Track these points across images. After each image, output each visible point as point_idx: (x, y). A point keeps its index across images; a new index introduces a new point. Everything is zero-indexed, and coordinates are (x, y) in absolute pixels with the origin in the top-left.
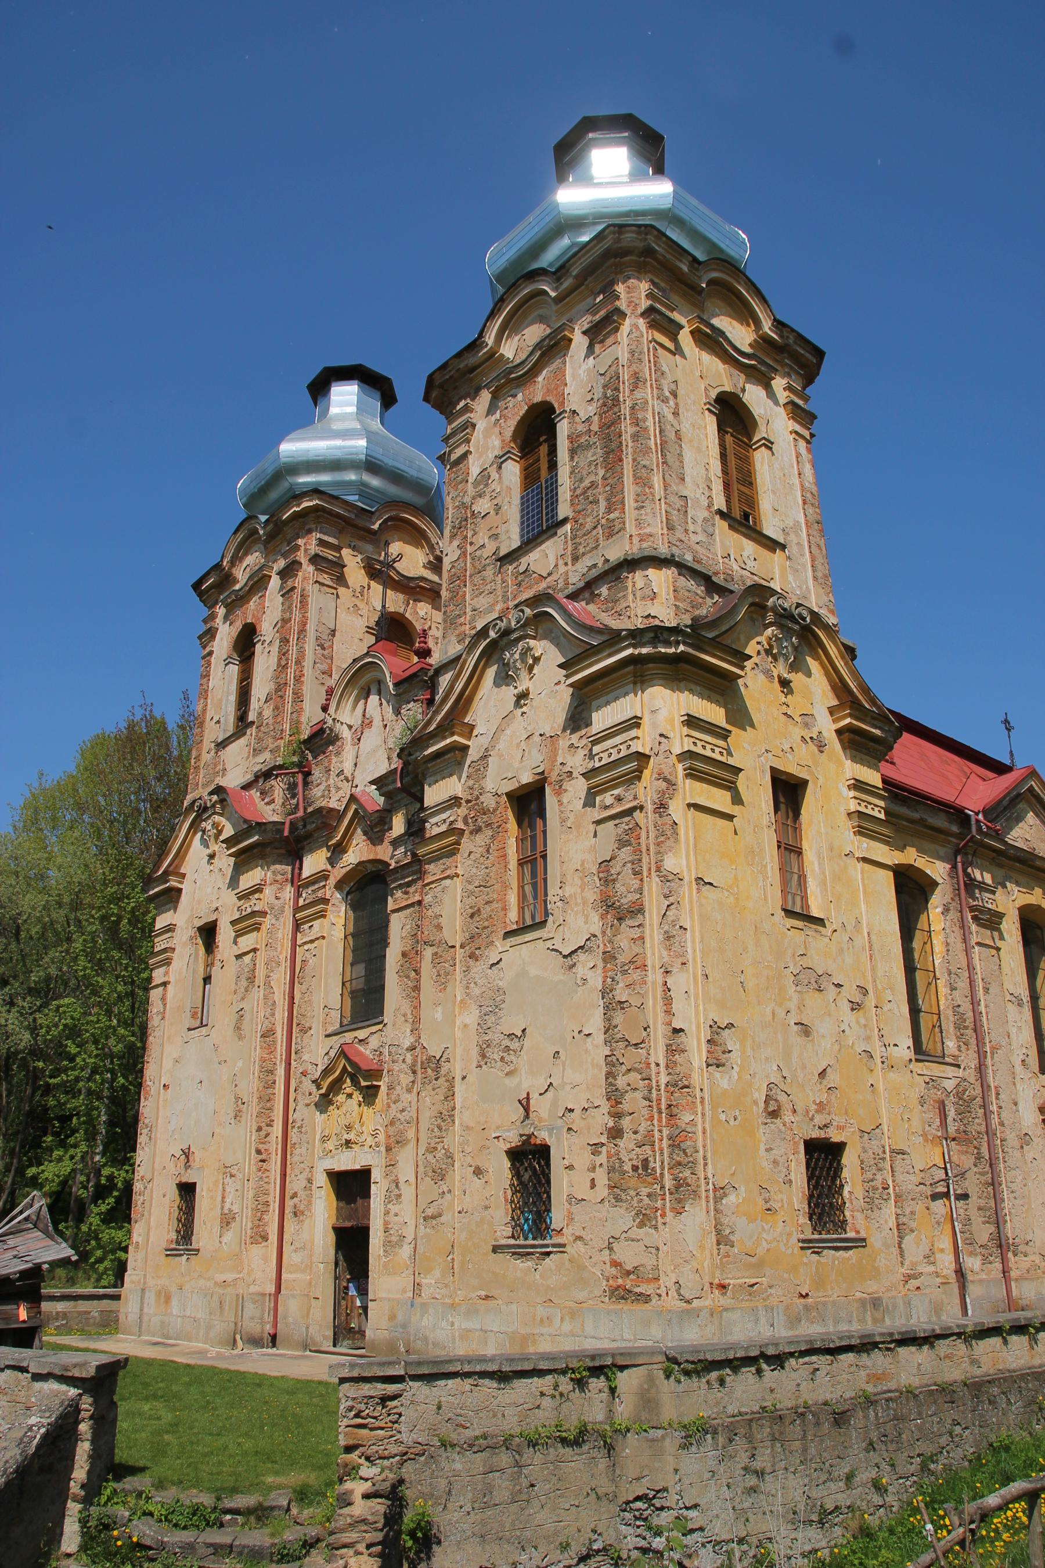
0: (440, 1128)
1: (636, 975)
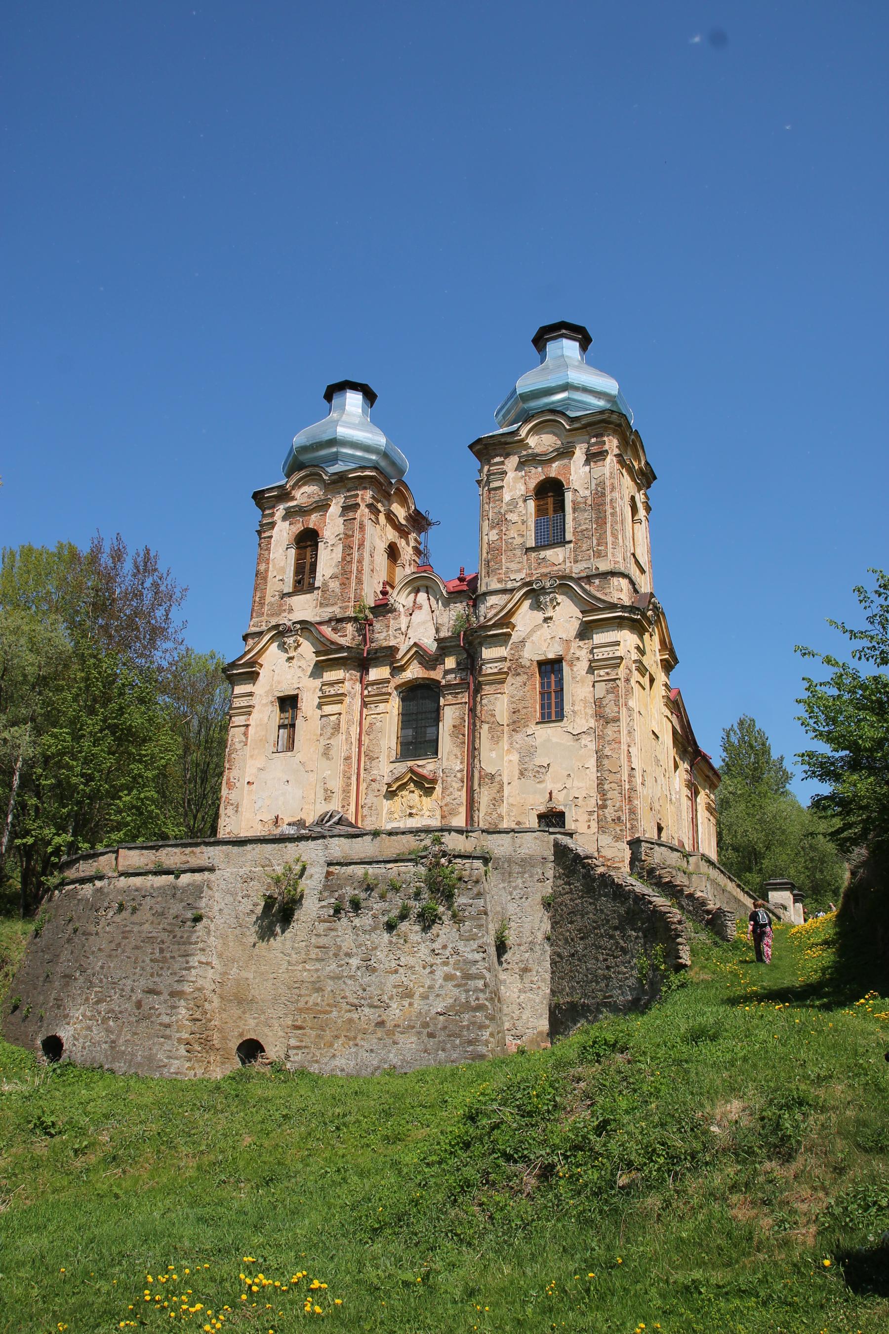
1: (616, 746)
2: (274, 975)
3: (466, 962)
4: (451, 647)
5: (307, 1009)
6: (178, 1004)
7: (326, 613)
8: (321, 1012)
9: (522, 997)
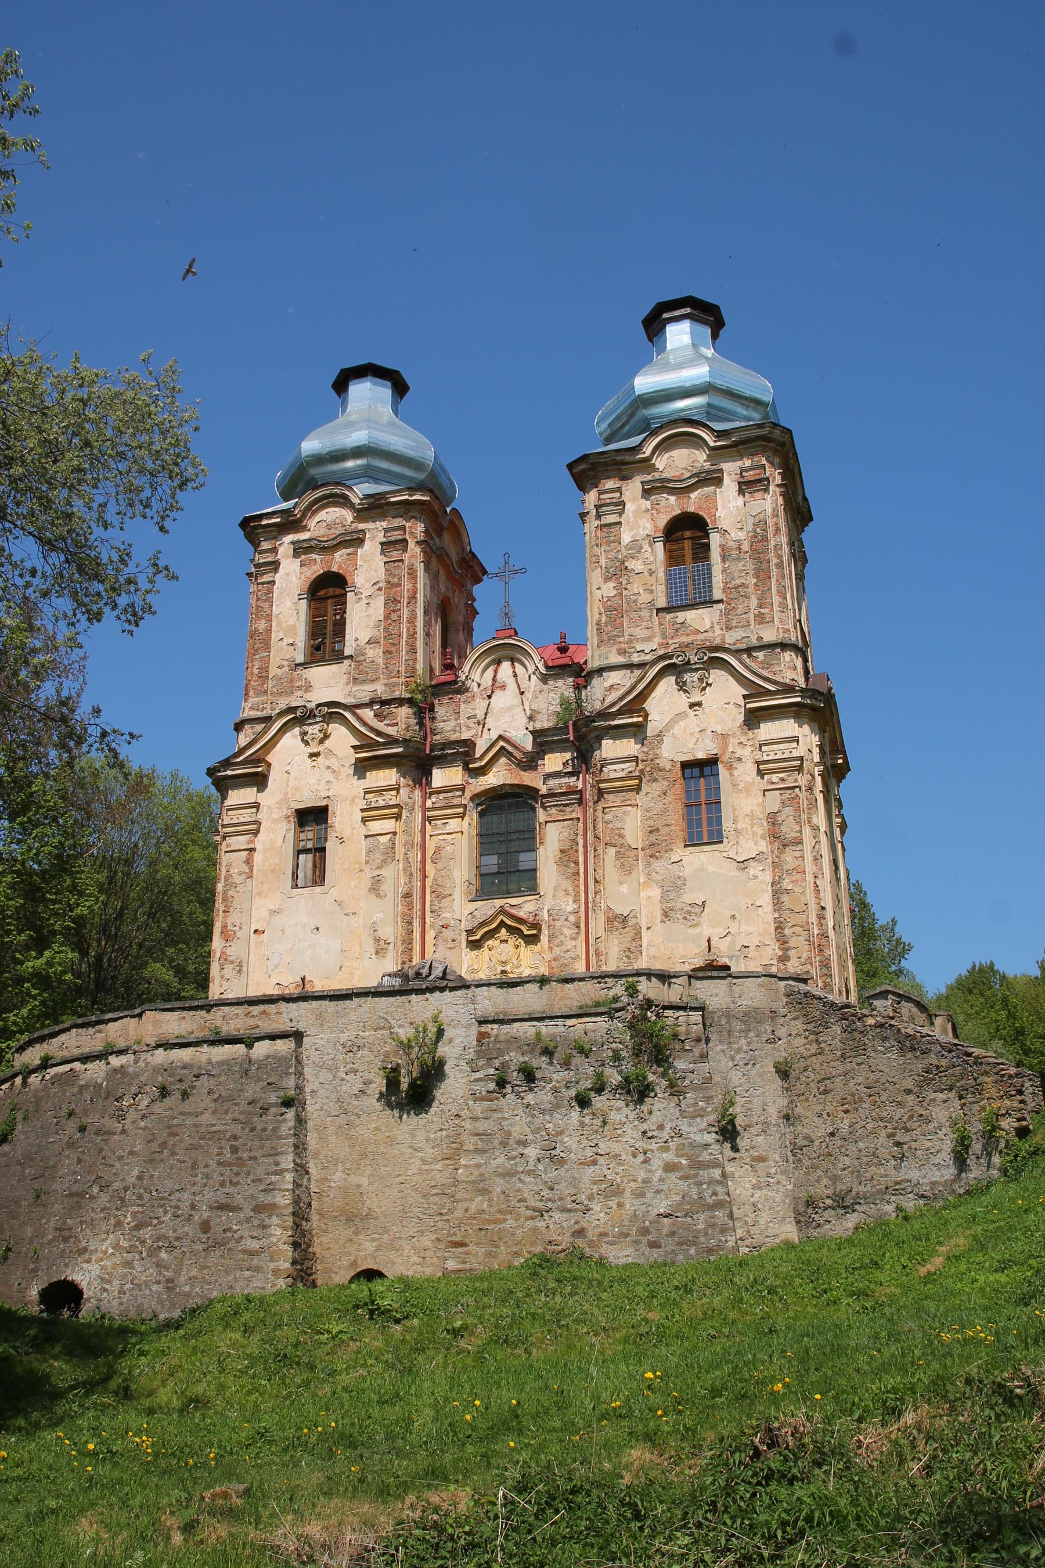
0: (628, 957)
2: (400, 1179)
3: (693, 1145)
4: (554, 742)
5: (469, 1218)
6: (267, 1222)
7: (365, 692)
8: (489, 1222)
9: (757, 1195)
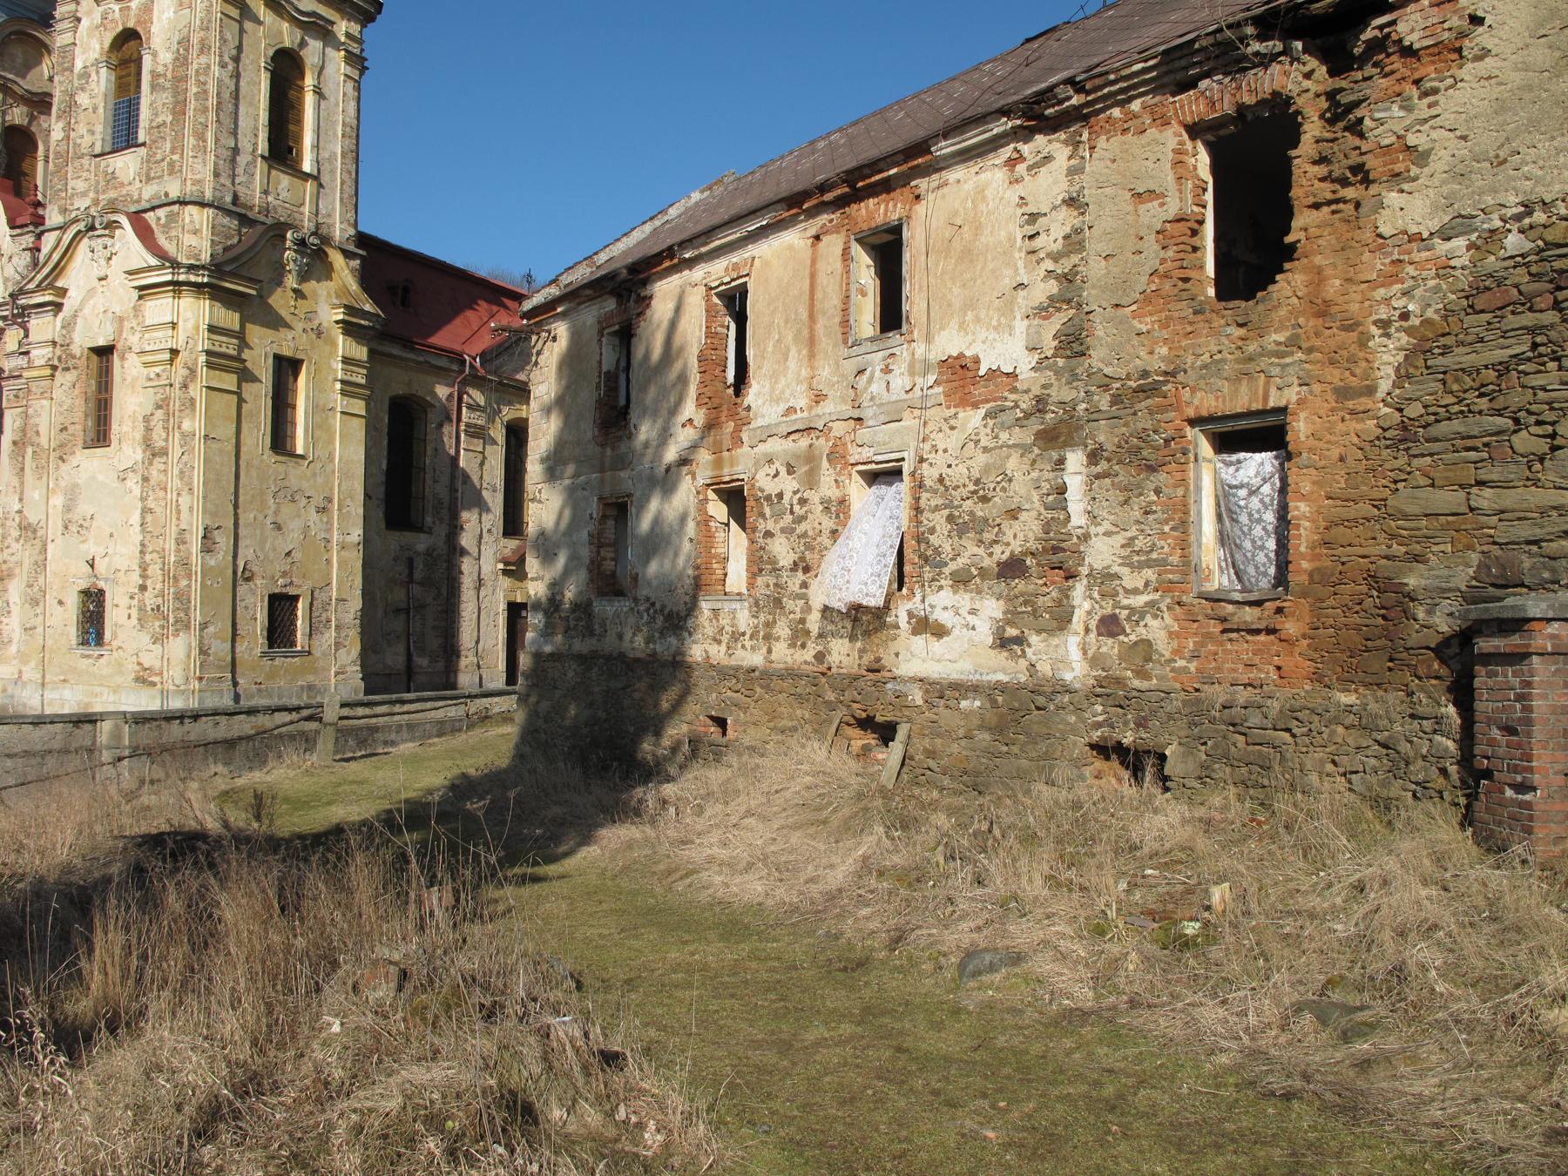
1: (161, 494)
